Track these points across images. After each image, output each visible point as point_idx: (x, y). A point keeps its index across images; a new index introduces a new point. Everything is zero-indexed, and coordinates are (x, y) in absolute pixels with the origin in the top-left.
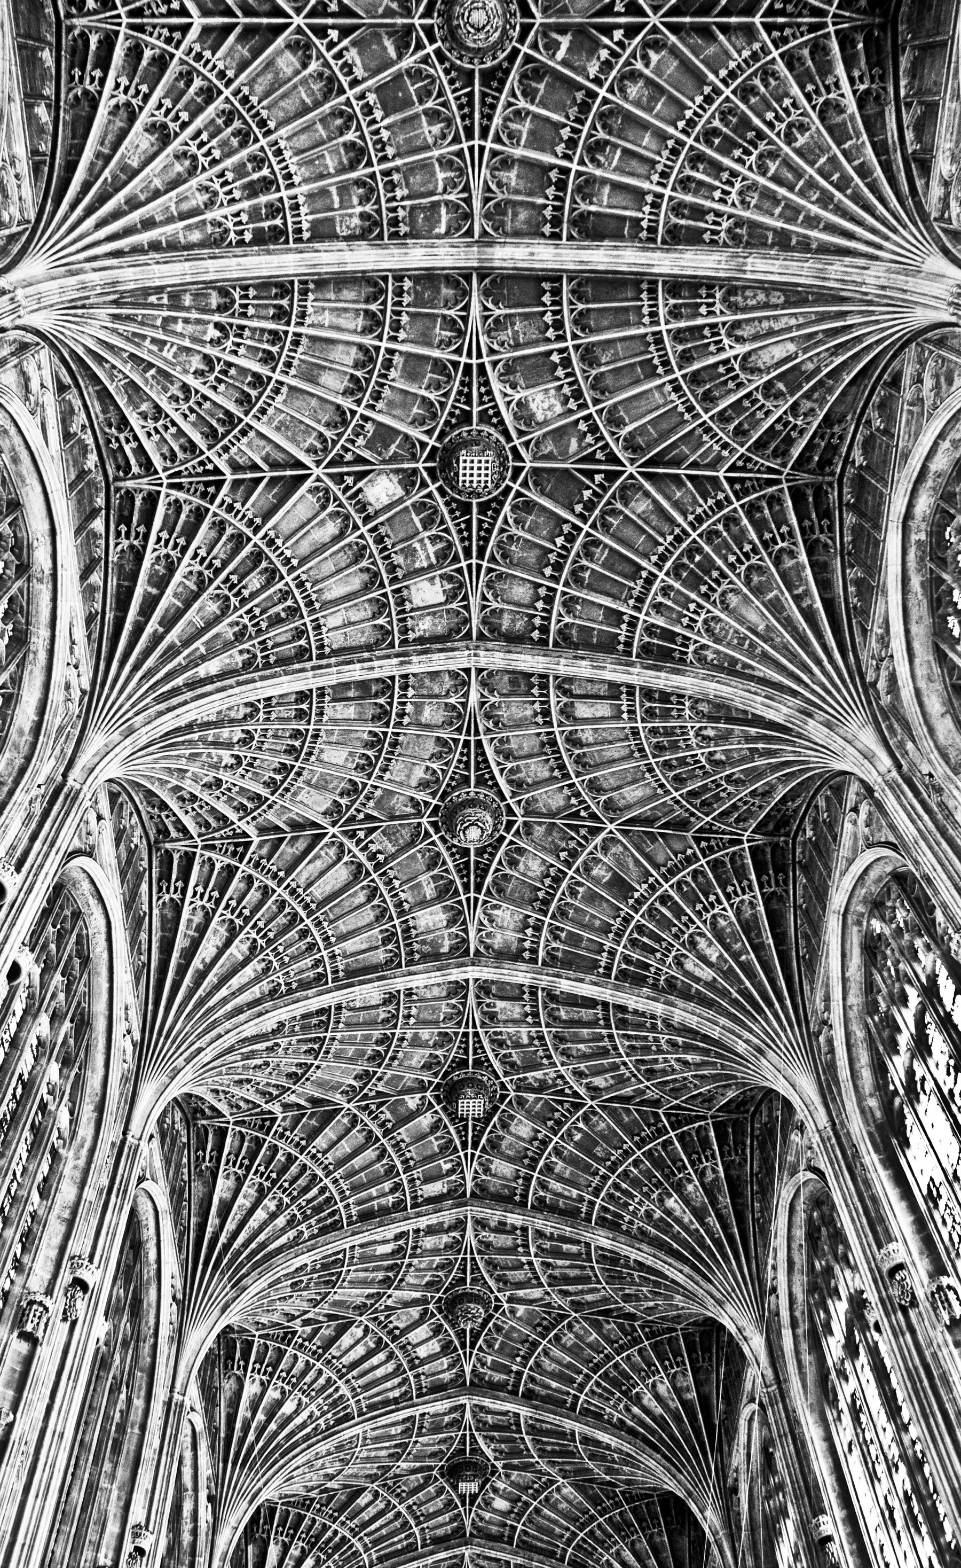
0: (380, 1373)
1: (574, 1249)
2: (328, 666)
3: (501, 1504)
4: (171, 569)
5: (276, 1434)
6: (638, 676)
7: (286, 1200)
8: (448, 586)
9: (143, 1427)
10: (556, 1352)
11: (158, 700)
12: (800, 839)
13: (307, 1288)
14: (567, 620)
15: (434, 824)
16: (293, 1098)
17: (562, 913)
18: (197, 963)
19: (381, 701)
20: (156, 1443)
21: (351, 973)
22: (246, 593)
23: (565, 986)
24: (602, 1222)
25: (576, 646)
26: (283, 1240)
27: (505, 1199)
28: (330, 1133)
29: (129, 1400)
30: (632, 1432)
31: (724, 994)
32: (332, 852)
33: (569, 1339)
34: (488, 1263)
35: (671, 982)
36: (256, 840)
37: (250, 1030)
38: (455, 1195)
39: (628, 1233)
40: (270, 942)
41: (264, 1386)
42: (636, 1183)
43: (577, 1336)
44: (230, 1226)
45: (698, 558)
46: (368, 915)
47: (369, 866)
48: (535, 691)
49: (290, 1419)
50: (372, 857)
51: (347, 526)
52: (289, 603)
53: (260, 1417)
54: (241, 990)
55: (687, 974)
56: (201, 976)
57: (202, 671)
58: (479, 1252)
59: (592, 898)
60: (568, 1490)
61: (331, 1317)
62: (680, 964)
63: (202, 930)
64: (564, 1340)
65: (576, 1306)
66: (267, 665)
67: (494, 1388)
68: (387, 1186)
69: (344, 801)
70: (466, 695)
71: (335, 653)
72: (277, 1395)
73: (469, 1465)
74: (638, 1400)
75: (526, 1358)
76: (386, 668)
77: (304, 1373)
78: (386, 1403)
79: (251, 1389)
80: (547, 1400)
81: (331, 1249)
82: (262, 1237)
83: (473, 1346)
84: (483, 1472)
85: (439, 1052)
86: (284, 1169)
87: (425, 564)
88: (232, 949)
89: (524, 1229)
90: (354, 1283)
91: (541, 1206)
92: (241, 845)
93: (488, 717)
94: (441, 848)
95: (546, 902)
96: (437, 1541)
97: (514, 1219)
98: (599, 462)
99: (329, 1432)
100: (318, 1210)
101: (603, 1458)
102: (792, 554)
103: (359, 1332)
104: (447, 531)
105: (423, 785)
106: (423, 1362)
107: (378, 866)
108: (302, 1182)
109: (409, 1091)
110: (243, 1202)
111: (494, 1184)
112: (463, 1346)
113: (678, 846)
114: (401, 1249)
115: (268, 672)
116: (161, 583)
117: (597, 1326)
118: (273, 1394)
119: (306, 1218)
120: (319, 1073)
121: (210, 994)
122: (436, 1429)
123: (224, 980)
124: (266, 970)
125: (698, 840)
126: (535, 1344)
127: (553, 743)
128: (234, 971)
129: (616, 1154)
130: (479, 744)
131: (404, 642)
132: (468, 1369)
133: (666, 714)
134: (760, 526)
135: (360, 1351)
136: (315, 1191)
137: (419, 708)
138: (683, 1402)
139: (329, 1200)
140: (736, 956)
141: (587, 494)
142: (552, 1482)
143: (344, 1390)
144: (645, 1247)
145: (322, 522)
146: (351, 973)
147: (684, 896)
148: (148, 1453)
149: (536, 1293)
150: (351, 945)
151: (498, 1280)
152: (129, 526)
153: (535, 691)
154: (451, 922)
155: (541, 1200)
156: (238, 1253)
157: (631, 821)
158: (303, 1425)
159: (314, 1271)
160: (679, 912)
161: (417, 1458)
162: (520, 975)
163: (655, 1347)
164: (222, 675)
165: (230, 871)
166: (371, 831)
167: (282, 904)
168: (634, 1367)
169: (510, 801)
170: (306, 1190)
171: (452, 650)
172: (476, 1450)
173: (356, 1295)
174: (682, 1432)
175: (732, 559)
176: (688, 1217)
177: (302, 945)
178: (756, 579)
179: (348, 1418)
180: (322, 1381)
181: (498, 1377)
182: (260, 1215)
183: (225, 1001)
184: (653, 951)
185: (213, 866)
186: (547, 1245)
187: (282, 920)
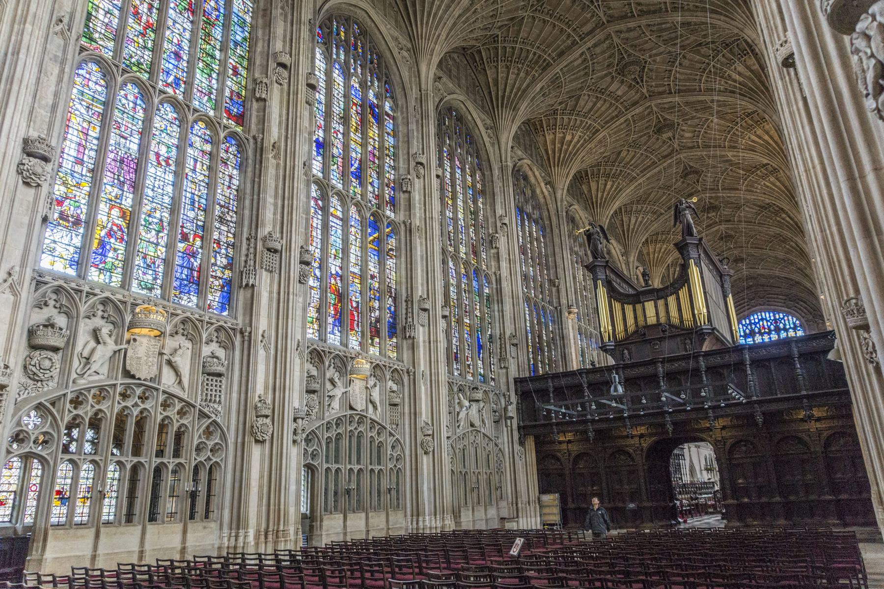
0: (603, 109)
1: (668, 25)
5: (567, 149)
7: (520, 66)
9: (492, 182)
13: (550, 93)
16: (500, 24)
20: (501, 184)
26: (527, 81)
27: (623, 17)
29: (483, 174)
30: (732, 92)
33: (686, 63)
34: (632, 46)
37: (456, 13)
38: (600, 25)
39: (689, 10)
43: (689, 60)
44: (501, 87)
49: (571, 142)
53: (558, 145)
58: (624, 44)
61: (570, 98)
64: (684, 64)
67: (660, 93)
68: (564, 37)
72: (561, 135)
73: (665, 126)
75: (669, 78)
77: (569, 123)
78: (613, 118)
79: (549, 138)
80: (685, 91)
81: (550, 75)
82: (517, 85)
83: (642, 81)
84: (671, 126)
89: (640, 26)
90: (571, 82)
91: (642, 13)
97: (632, 25)
99: (591, 139)
100: (537, 62)
101: (725, 105)
103: (586, 97)
106: (621, 97)
111: (616, 13)
112: (638, 83)
114: (585, 60)
117: (698, 53)
118: (559, 135)
119: (533, 69)
120: (504, 9)
122: (643, 118)
126: (671, 71)
132: (645, 91)
135: (590, 104)
136: (531, 56)
138: (752, 71)
139: (540, 56)
142: (708, 119)
143: (589, 122)
144: (699, 14)
148: (497, 190)
149: (662, 49)
151: (640, 50)
155: (641, 11)
156: (510, 96)
158: (578, 141)
159: (549, 86)
161: (639, 132)
163: (731, 52)
168: (722, 64)
170: (527, 57)
172: (665, 120)
174: (755, 85)
179: (597, 131)
180: (578, 122)
181: (661, 89)
182: (512, 77)
186: (655, 28)
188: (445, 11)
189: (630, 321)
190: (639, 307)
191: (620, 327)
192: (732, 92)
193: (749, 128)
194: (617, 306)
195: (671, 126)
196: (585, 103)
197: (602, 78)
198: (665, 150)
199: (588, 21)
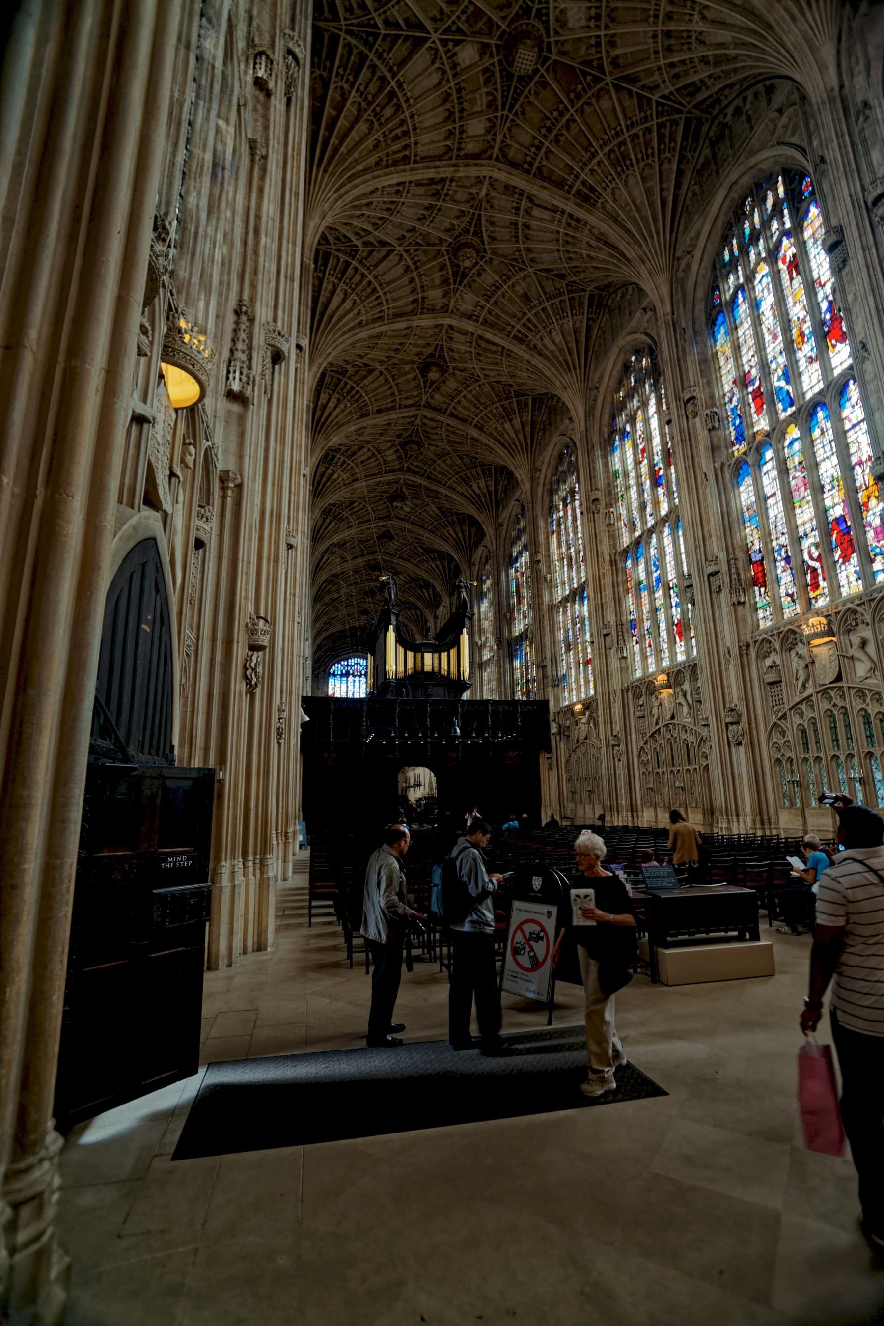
2: (417, 169)
3: (407, 509)
4: (344, 99)
6: (570, 207)
8: (488, 124)
10: (442, 465)
11: (335, 192)
12: (613, 296)
14: (544, 163)
15: (447, 251)
17: (496, 303)
18: (329, 312)
19: (438, 187)
21: (396, 316)
22: (383, 120)
23: (488, 336)
24: (476, 426)
25: (544, 178)
28: (370, 378)
30: (466, 497)
31: (556, 357)
32: (397, 258)
35: (535, 346)
36: (361, 248)
40: (362, 301)
41: (327, 469)
42: (493, 415)
44: (325, 415)
45: (623, 148)
46: (408, 289)
47: (412, 267)
48: (516, 196)
50: (415, 263)
51: (442, 79)
52: (404, 128)
53: (324, 479)
54: (347, 323)
55: (544, 345)
56: (331, 317)
57: (354, 171)
59: (511, 299)
60: (434, 509)
62: (541, 339)
63: (333, 293)
65: (455, 451)
66: (387, 166)
69: (408, 235)
70: (481, 189)
71: (424, 159)
74: (471, 487)
76: (447, 172)
81: (364, 425)
85: (424, 350)
86: (349, 393)
87: (479, 109)
88: (345, 304)
91: (452, 415)
92: (353, 252)
93: (488, 202)
94: (448, 263)
95: (490, 297)
96: (380, 518)
98: (592, 67)
100: (360, 409)
102: (670, 161)
104: (496, 90)
105: (447, 230)
107: (417, 268)
108: (357, 397)
109: (407, 364)
110: (331, 405)
111: (434, 403)
113: (558, 286)
115: (387, 170)
116: (339, 108)
117: (461, 458)
121: (334, 326)
123: (339, 320)
124: (359, 313)
125: (567, 285)
127: (516, 225)
128: (344, 316)
129: (489, 403)
130: (480, 215)
131: (458, 156)
133: (576, 229)
134: (661, 137)
135: (365, 457)
137: (455, 191)
140: (567, 343)
141: (580, 87)
145: (429, 75)
146: (396, 316)
147: (553, 309)
150: (396, 304)
152: (320, 59)
153: (516, 196)
154: (444, 296)
157: (540, 270)
160: (548, 317)
162: (469, 326)
163: (483, 470)
164: (365, 171)
165: (347, 264)
166: (416, 250)
167: (370, 283)
169: (487, 247)
170: (357, 401)
171: (482, 165)
172: (401, 491)
173: (368, 438)
175: (640, 156)
176: (512, 433)
177: (376, 303)
178: (647, 171)
179: (357, 480)
181: (417, 470)
182: (338, 410)
183: (340, 329)
184: (532, 331)
185: (339, 260)
187: (369, 290)
188: (342, 335)
189: (410, 665)
190: (419, 655)
191: (401, 669)
192: (466, 497)
193: (452, 524)
194: (401, 650)
195: (402, 498)
196: (361, 456)
197: (386, 441)
198: (384, 513)
199: (412, 397)
